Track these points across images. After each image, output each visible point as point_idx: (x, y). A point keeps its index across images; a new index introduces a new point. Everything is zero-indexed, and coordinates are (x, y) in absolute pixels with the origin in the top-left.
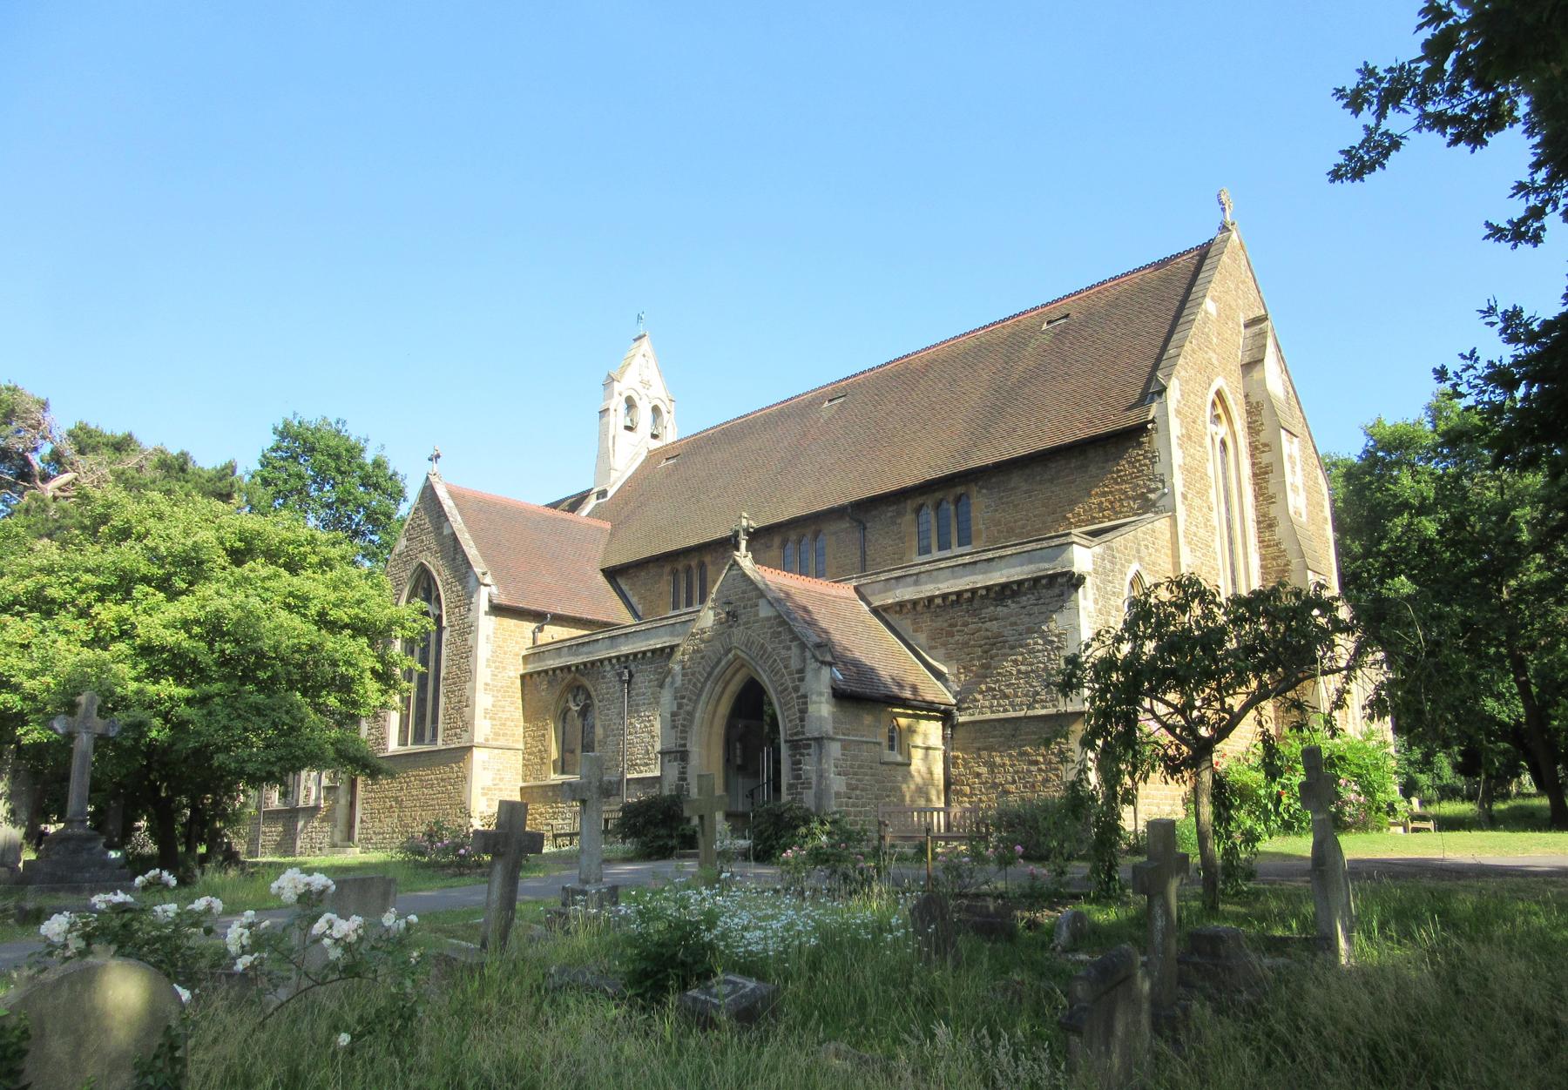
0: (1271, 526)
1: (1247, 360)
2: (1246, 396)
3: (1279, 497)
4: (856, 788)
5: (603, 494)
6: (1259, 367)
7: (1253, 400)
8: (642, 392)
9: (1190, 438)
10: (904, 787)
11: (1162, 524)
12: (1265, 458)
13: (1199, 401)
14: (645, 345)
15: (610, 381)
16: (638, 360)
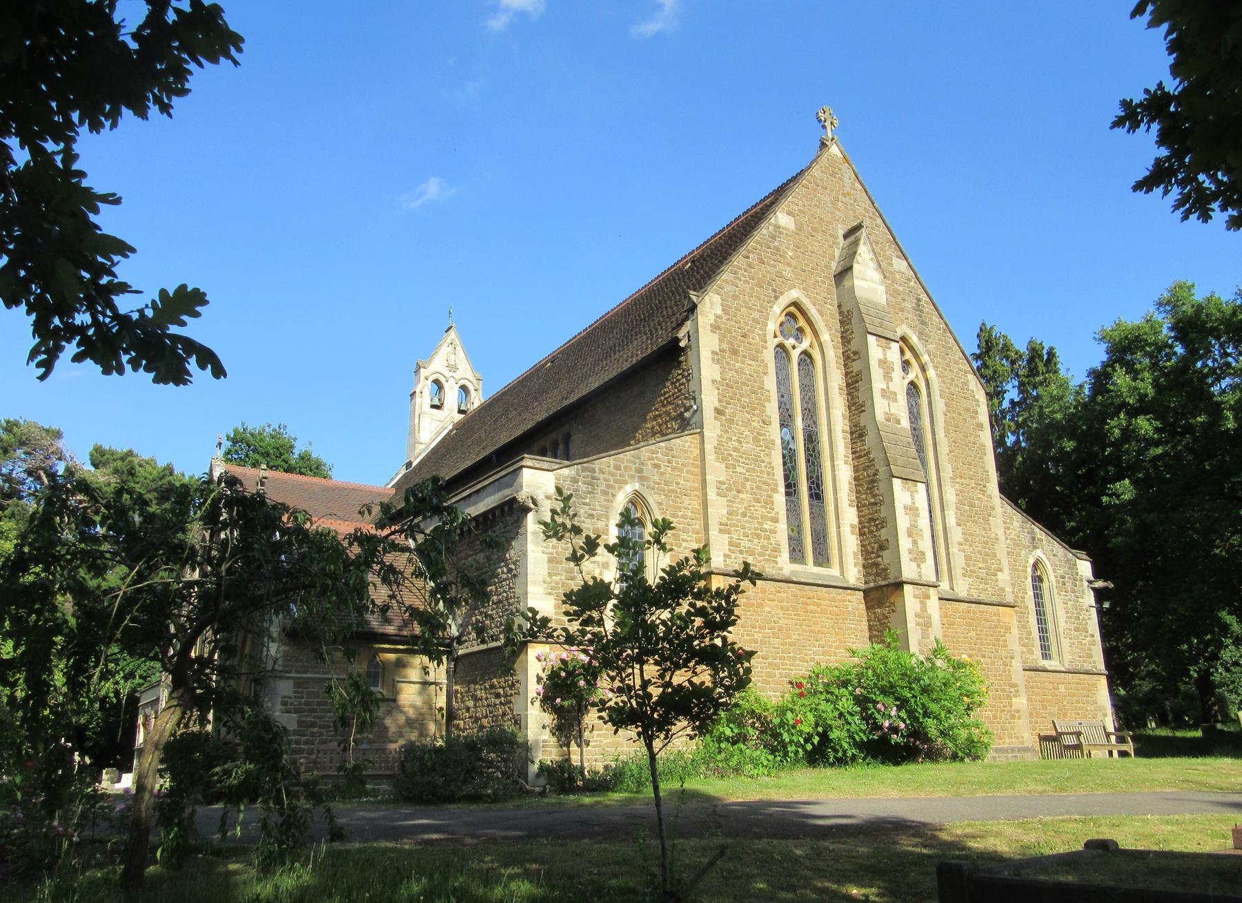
0: (861, 435)
1: (840, 269)
2: (839, 306)
3: (868, 404)
4: (313, 725)
5: (409, 464)
6: (849, 275)
7: (844, 309)
8: (448, 374)
9: (734, 352)
10: (388, 722)
11: (685, 443)
12: (856, 366)
13: (756, 315)
14: (452, 335)
15: (419, 367)
16: (445, 350)
